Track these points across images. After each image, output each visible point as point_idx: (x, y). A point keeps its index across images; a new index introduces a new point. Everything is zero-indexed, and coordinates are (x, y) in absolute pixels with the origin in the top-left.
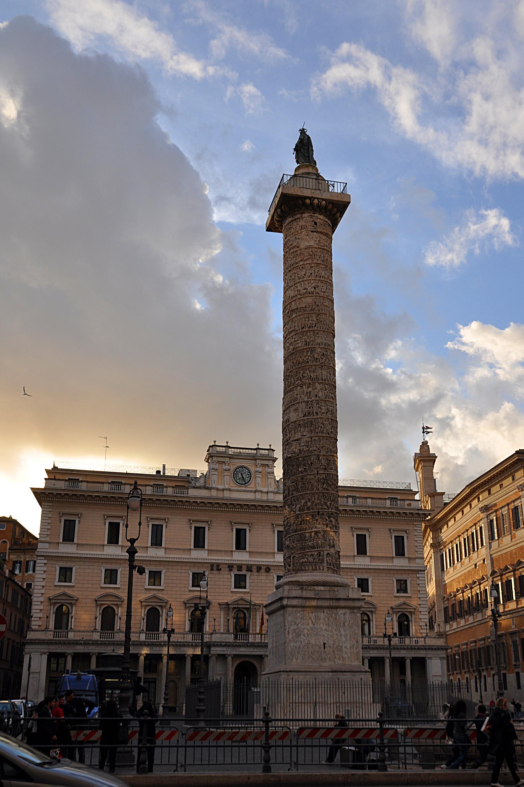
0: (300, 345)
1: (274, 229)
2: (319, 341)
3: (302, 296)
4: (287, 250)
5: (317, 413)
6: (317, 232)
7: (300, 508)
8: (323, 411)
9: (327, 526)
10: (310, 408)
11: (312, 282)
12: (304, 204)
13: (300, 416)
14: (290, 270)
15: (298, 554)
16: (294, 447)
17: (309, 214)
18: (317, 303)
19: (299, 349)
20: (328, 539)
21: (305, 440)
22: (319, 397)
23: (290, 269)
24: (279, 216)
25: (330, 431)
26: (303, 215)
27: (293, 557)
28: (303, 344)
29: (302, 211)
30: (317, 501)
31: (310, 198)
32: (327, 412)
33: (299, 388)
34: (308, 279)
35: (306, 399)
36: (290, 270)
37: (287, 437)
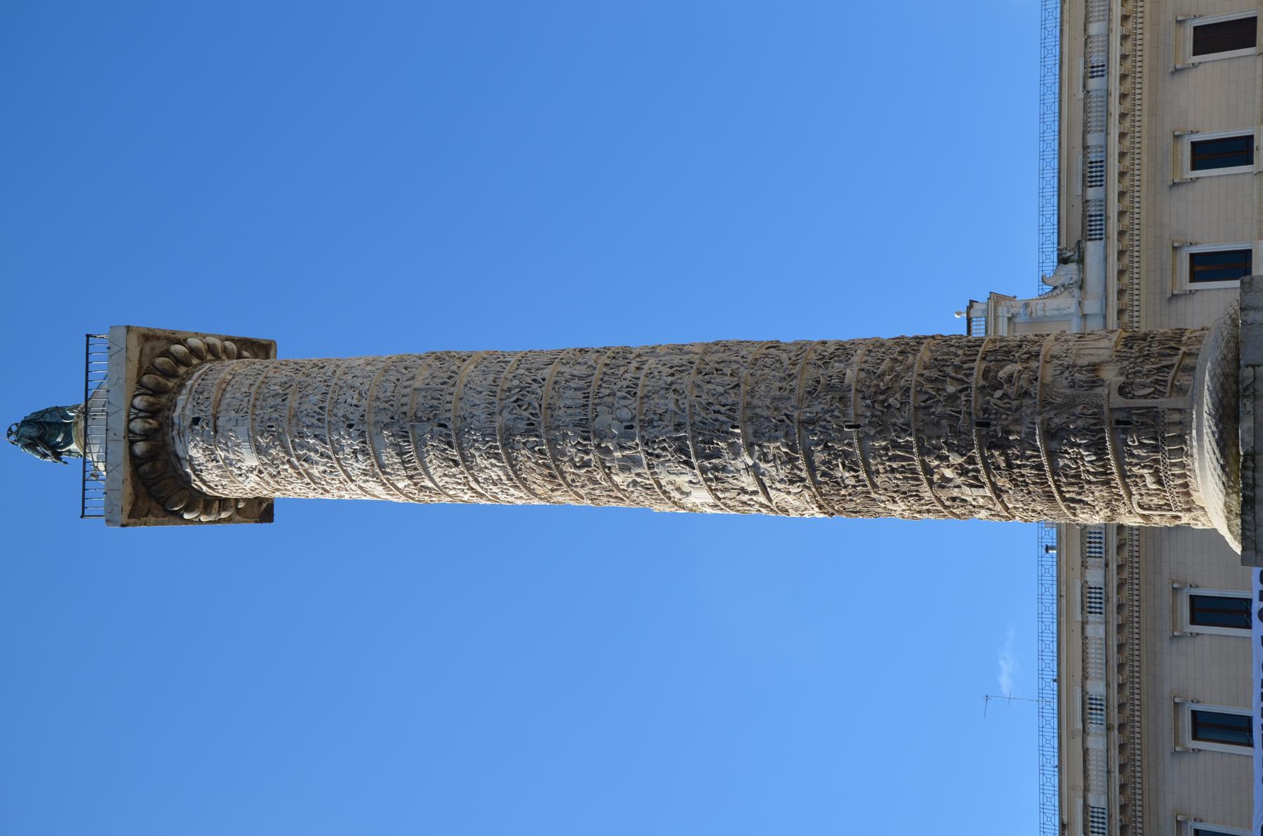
2: (483, 416)
5: (679, 426)
6: (216, 418)
7: (971, 486)
8: (672, 406)
9: (1026, 394)
10: (664, 449)
12: (151, 456)
16: (783, 495)
17: (177, 440)
18: (387, 420)
19: (511, 473)
20: (1068, 391)
22: (633, 418)
24: (207, 510)
25: (728, 379)
26: (181, 454)
29: (173, 459)
31: (132, 443)
32: (675, 391)
33: (615, 478)
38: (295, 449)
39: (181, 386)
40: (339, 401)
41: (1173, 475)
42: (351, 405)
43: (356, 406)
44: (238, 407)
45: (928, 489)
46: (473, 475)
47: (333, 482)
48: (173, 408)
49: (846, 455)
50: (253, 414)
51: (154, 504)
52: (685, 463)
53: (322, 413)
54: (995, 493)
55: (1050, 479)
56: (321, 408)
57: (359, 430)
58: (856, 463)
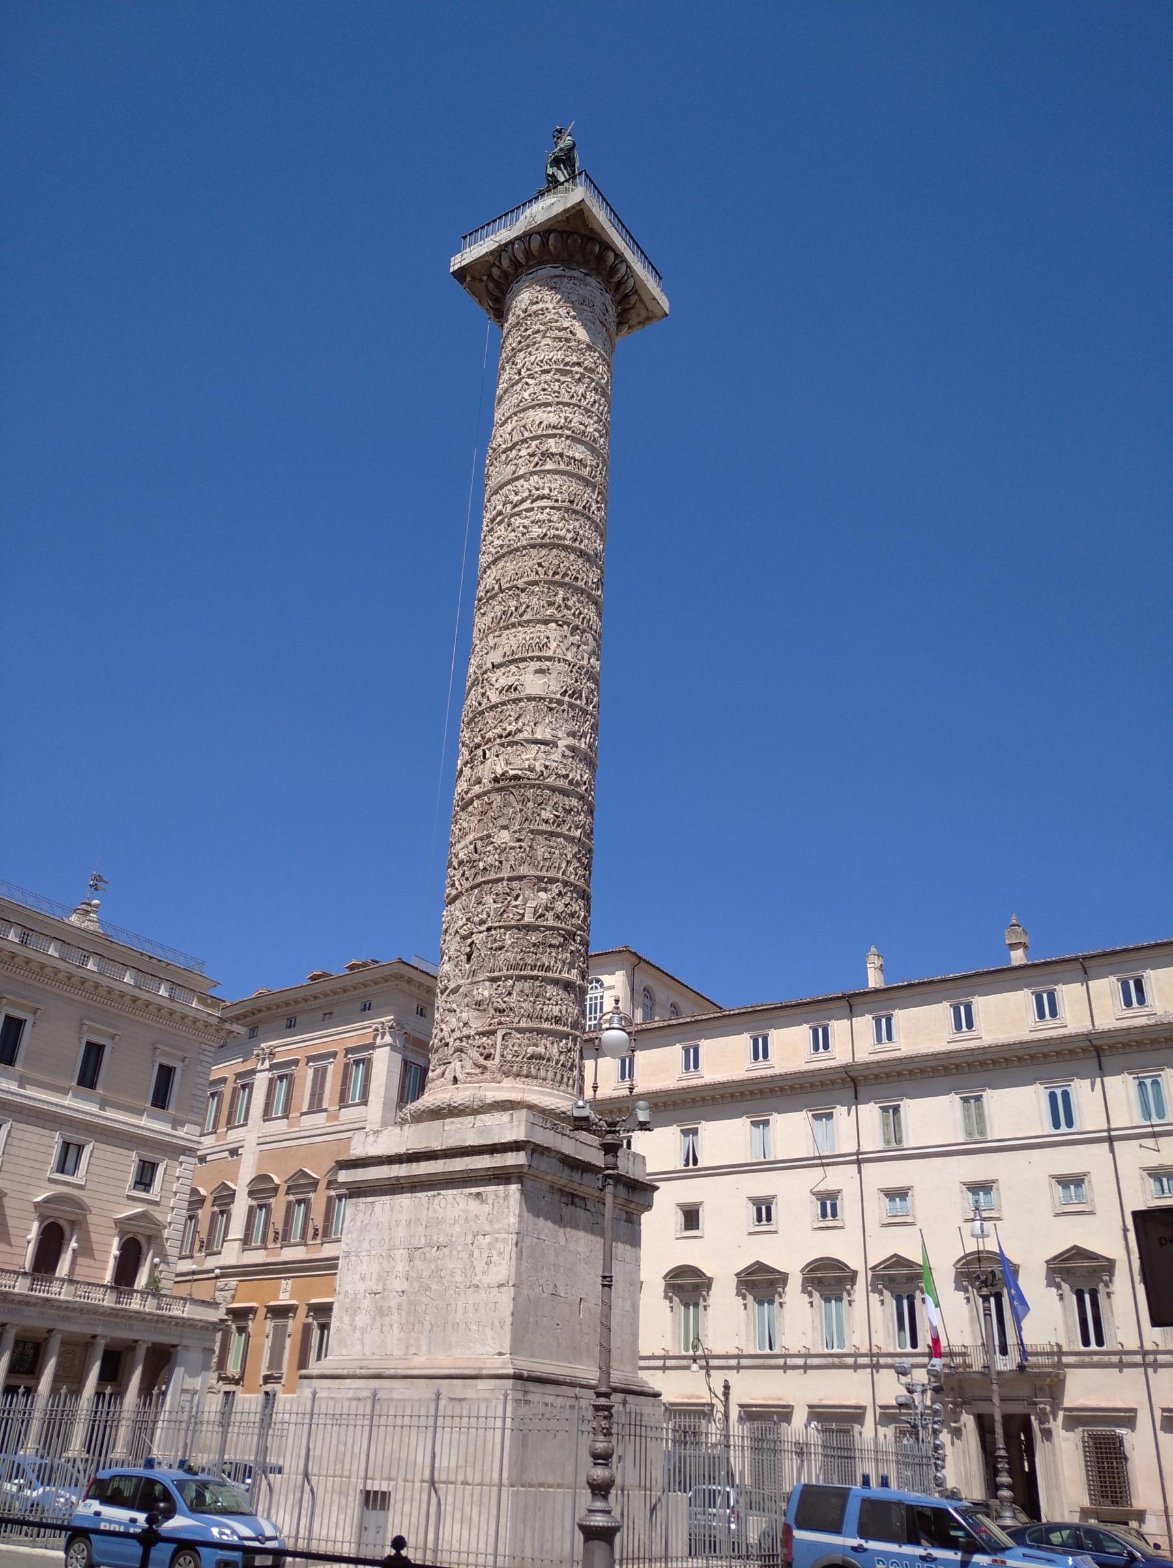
0: (562, 533)
1: (473, 278)
4: (542, 328)
7: (535, 911)
10: (576, 681)
12: (601, 258)
13: (552, 688)
14: (548, 372)
15: (520, 1031)
21: (560, 750)
23: (547, 367)
26: (588, 279)
27: (504, 1036)
28: (569, 535)
30: (575, 907)
35: (569, 657)
36: (548, 372)
37: (509, 728)
41: (539, 1069)
45: (532, 873)
46: (558, 509)
49: (564, 821)
51: (568, 229)
52: (566, 691)
54: (528, 926)
55: (540, 974)
58: (559, 825)
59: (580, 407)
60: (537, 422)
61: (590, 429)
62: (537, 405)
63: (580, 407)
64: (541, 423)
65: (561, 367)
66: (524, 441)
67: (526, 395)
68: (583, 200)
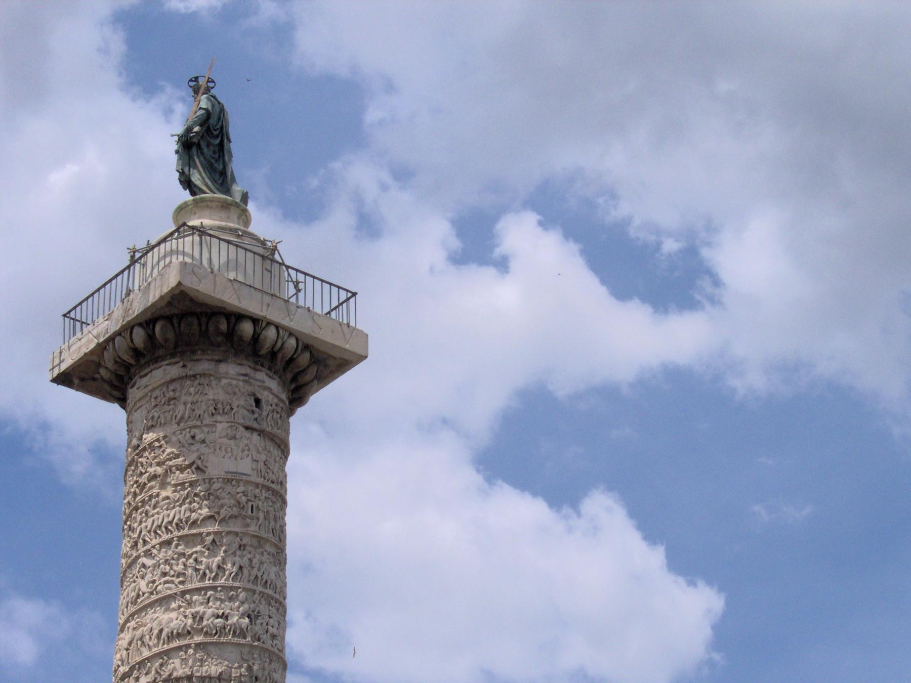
1: (82, 380)
3: (208, 640)
4: (159, 470)
6: (261, 433)
11: (242, 595)
12: (231, 335)
14: (168, 543)
23: (165, 537)
26: (223, 368)
31: (255, 321)
34: (230, 583)
38: (229, 533)
39: (283, 384)
40: (271, 607)
42: (267, 624)
43: (267, 632)
44: (269, 466)
47: (181, 567)
48: (271, 374)
50: (263, 486)
51: (175, 311)
53: (262, 584)
56: (266, 582)
57: (247, 629)
59: (214, 588)
60: (156, 632)
61: (234, 619)
62: (156, 601)
63: (214, 588)
64: (161, 631)
65: (186, 531)
66: (141, 664)
67: (143, 585)
68: (180, 284)
